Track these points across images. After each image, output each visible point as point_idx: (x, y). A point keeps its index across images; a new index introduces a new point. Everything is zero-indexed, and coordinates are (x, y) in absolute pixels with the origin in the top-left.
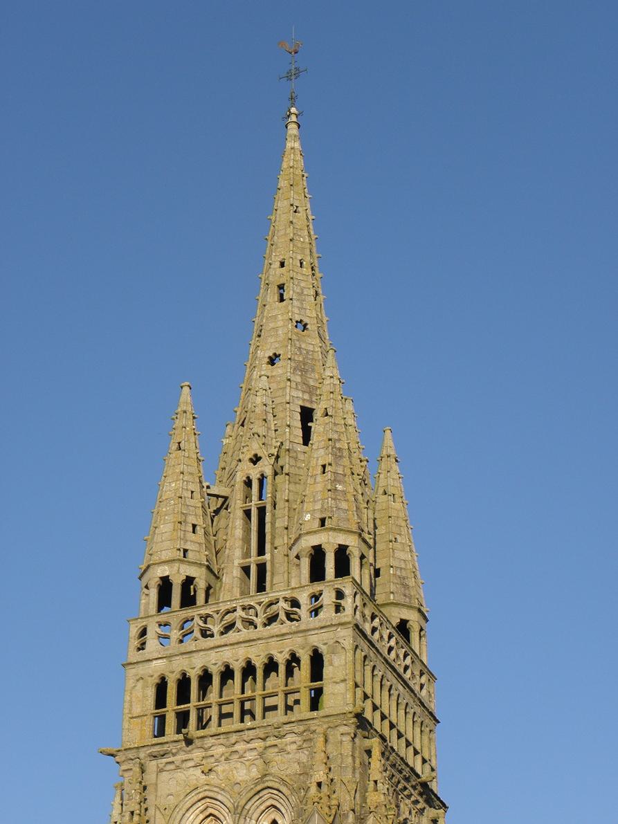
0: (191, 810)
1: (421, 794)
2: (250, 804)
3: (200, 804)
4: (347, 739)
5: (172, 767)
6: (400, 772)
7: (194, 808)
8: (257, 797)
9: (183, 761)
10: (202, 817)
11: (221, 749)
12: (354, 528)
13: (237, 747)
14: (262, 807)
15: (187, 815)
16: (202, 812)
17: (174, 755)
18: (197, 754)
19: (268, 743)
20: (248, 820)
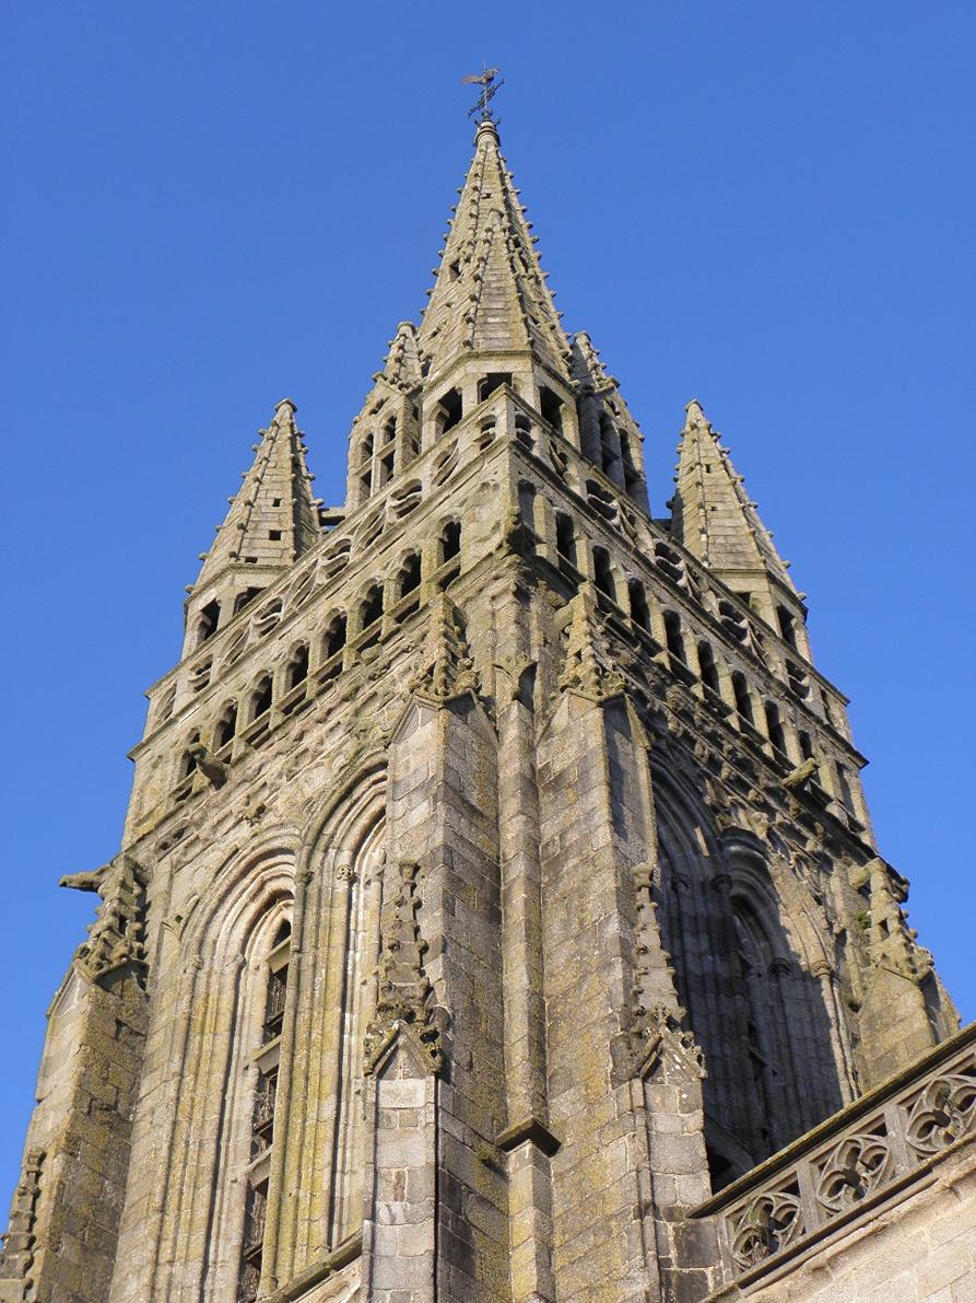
0: (231, 899)
1: (807, 822)
2: (334, 821)
3: (246, 881)
4: (507, 607)
5: (197, 849)
6: (713, 738)
7: (236, 891)
8: (347, 804)
9: (215, 828)
10: (254, 907)
11: (281, 762)
12: (522, 343)
13: (308, 742)
14: (364, 821)
15: (222, 912)
16: (253, 898)
17: (198, 825)
18: (239, 797)
19: (361, 698)
20: (332, 852)
